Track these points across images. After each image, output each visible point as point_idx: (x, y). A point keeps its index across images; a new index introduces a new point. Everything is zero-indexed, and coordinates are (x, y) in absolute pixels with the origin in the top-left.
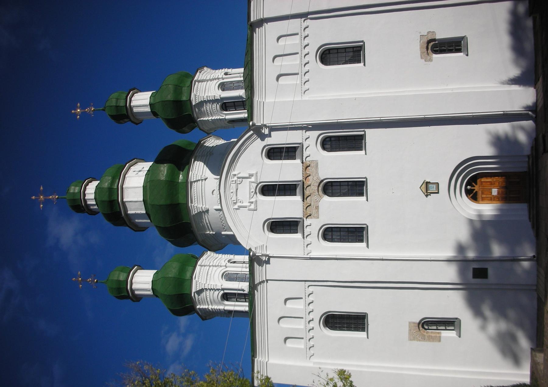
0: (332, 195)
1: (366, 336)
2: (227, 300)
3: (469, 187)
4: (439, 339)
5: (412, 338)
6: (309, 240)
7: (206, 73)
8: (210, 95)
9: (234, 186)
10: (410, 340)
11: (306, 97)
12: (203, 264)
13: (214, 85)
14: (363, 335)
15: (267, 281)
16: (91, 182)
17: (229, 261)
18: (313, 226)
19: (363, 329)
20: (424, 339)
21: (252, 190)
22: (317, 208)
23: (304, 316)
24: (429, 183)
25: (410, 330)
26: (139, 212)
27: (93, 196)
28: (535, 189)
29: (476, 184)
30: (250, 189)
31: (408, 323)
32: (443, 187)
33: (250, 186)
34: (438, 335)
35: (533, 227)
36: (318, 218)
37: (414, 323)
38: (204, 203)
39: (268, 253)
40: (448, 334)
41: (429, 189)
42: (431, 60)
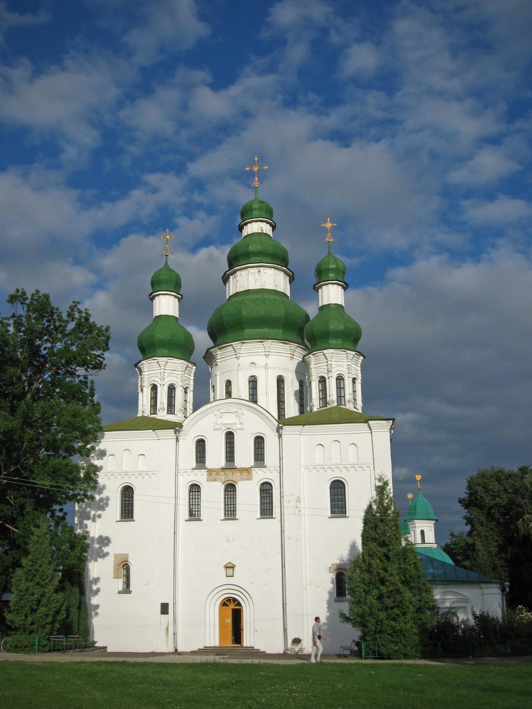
0: (226, 491)
2: (152, 389)
5: (116, 556)
9: (233, 410)
14: (118, 518)
16: (271, 225)
18: (200, 477)
19: (122, 518)
20: (115, 565)
22: (215, 480)
25: (122, 555)
30: (232, 424)
32: (230, 580)
36: (208, 481)
37: (128, 558)
38: (244, 355)
39: (180, 440)
40: (120, 584)
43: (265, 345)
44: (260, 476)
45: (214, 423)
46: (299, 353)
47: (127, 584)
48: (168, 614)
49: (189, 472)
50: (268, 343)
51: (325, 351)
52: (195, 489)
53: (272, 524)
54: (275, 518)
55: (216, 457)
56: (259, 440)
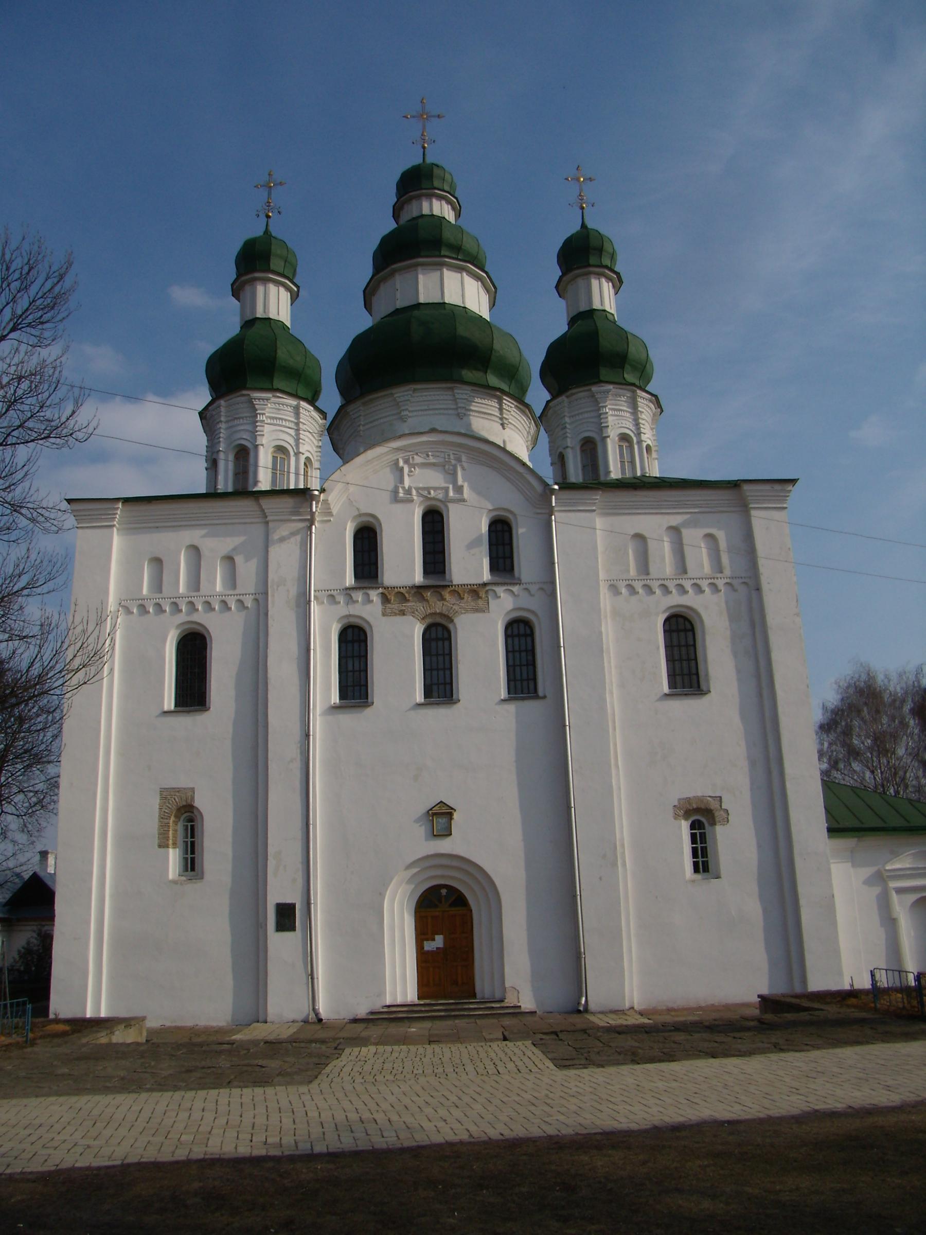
1: (166, 708)
3: (444, 891)
4: (163, 845)
5: (166, 794)
6: (341, 599)
7: (646, 409)
8: (610, 419)
10: (163, 791)
11: (604, 591)
12: (301, 410)
13: (627, 426)
14: (169, 702)
15: (267, 523)
16: (454, 209)
17: (308, 459)
20: (163, 817)
21: (432, 492)
22: (402, 613)
23: (202, 592)
24: (451, 819)
25: (178, 790)
26: (398, 295)
27: (426, 211)
28: (442, 1014)
29: (451, 905)
30: (435, 489)
31: (191, 786)
33: (442, 488)
34: (171, 842)
35: (372, 1013)
36: (384, 615)
37: (193, 798)
38: (415, 413)
42: (676, 816)
43: (457, 396)
44: (504, 604)
45: (396, 488)
48: (292, 928)
51: (594, 389)
54: (544, 697)
55: (403, 561)
56: (499, 527)
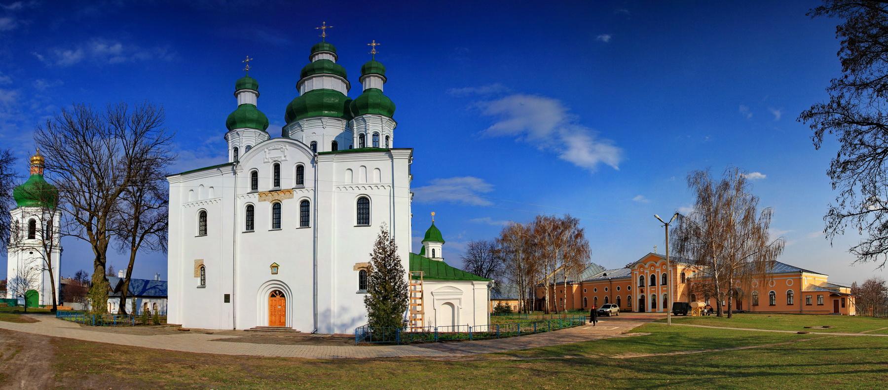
18: (254, 199)
32: (275, 277)
41: (275, 267)
44: (299, 195)
46: (345, 122)
47: (203, 280)
49: (245, 195)
50: (325, 120)
52: (250, 209)
53: (309, 232)
55: (266, 182)
